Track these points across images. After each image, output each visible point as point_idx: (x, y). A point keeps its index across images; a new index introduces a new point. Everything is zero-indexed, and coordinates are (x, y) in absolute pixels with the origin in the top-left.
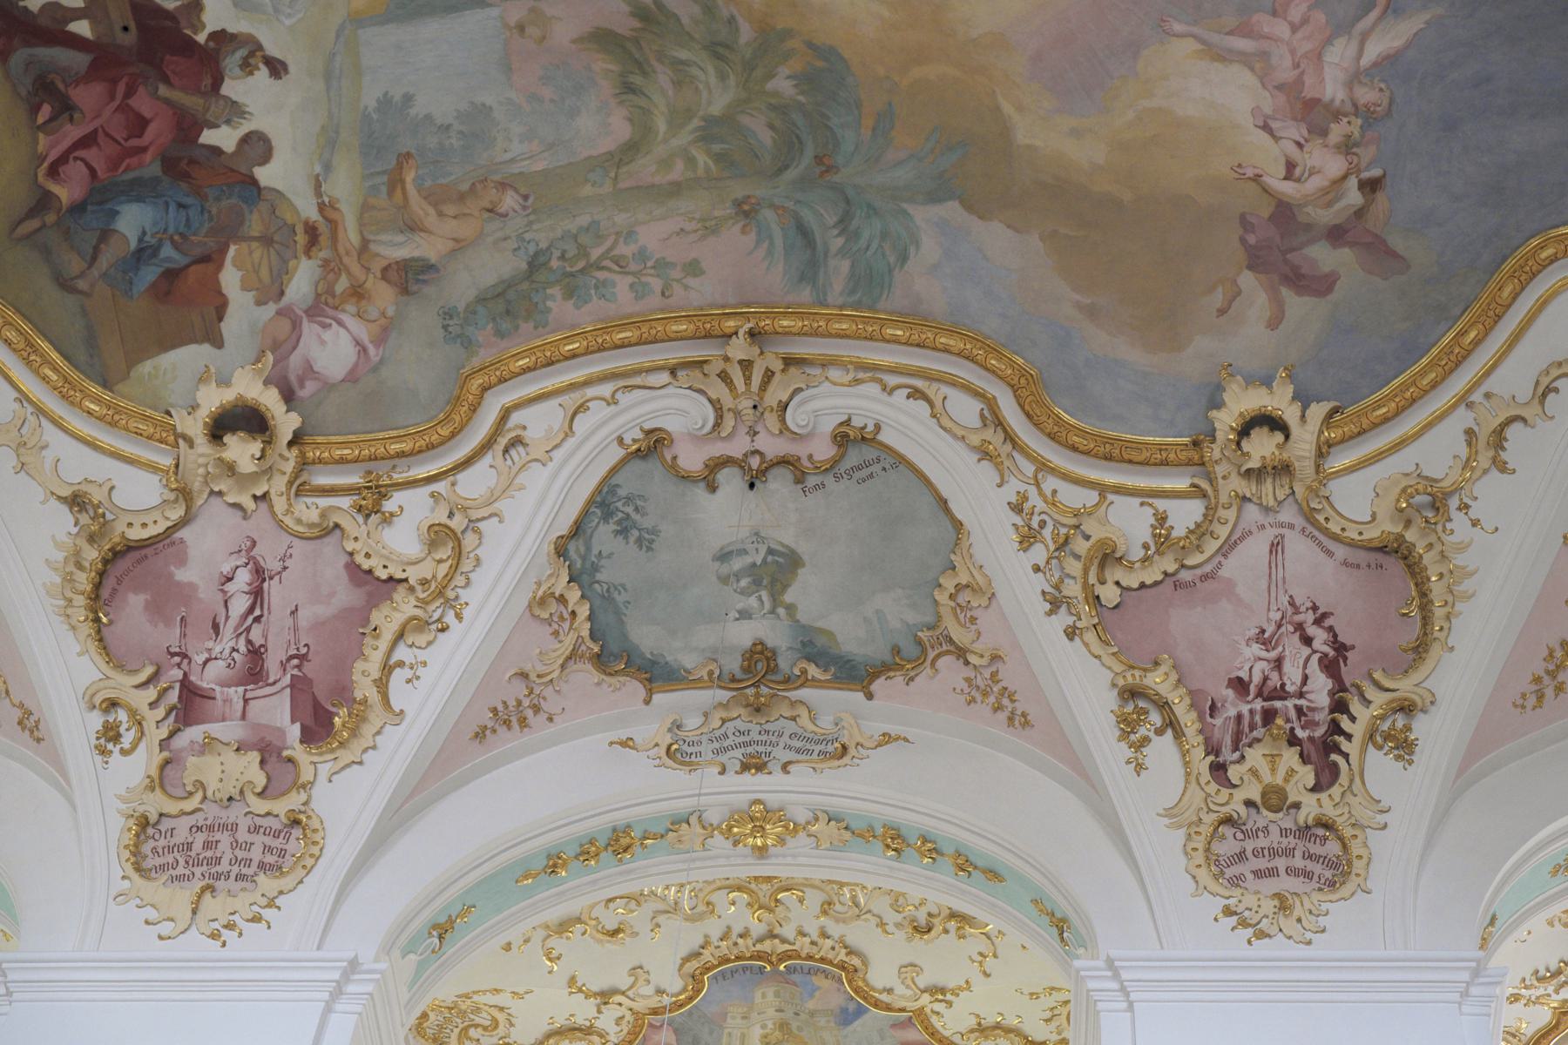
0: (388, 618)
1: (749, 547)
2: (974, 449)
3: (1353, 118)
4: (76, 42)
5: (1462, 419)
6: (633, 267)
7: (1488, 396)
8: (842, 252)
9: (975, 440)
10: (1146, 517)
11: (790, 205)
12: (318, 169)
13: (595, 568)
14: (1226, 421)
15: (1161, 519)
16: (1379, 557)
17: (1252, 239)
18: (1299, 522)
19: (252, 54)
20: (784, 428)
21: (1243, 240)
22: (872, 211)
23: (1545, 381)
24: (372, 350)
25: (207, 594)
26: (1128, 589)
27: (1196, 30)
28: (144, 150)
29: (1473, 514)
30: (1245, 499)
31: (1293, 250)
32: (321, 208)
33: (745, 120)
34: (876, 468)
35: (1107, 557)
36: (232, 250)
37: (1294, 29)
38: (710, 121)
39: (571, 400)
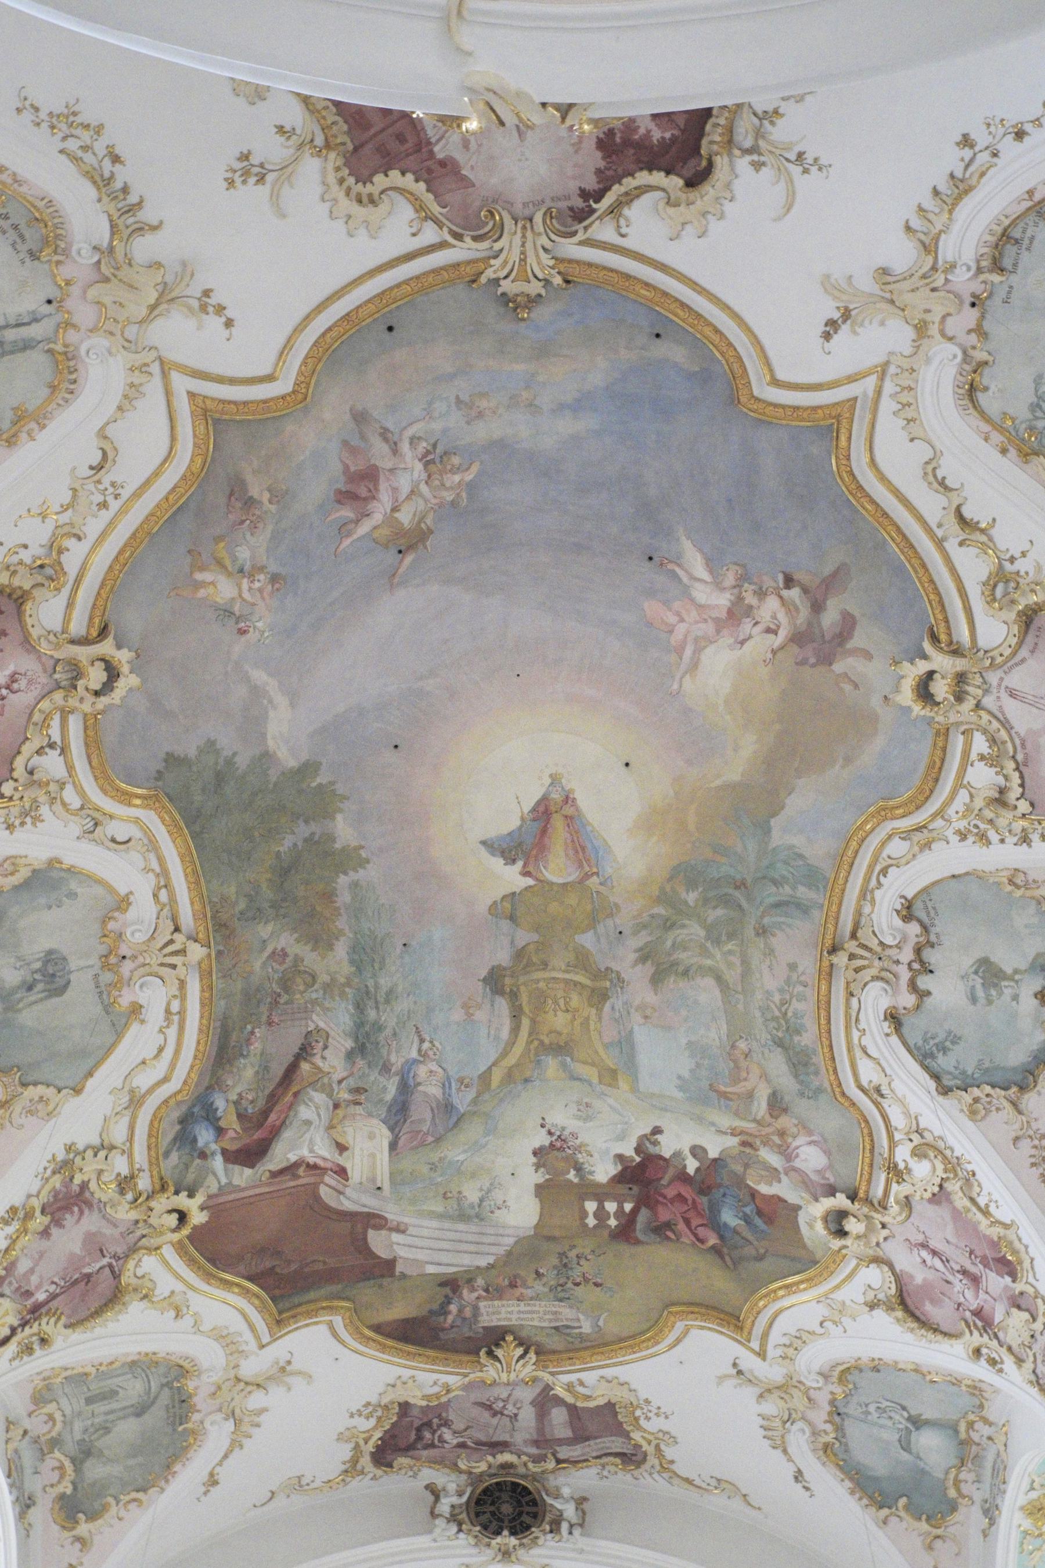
0: (961, 1202)
1: (971, 983)
2: (921, 850)
3: (743, 589)
4: (635, 1211)
5: (951, 546)
7: (940, 526)
8: (794, 888)
9: (916, 849)
10: (980, 766)
11: (761, 909)
12: (713, 1129)
13: (964, 1073)
14: (918, 709)
15: (982, 758)
16: (1033, 627)
17: (812, 660)
18: (999, 673)
20: (898, 946)
21: (813, 666)
22: (771, 866)
23: (936, 485)
25: (930, 1275)
26: (1023, 795)
28: (694, 1201)
29: (1017, 555)
30: (978, 706)
32: (733, 1134)
33: (709, 920)
34: (930, 904)
35: (1000, 799)
37: (682, 620)
38: (708, 938)
39: (858, 1053)
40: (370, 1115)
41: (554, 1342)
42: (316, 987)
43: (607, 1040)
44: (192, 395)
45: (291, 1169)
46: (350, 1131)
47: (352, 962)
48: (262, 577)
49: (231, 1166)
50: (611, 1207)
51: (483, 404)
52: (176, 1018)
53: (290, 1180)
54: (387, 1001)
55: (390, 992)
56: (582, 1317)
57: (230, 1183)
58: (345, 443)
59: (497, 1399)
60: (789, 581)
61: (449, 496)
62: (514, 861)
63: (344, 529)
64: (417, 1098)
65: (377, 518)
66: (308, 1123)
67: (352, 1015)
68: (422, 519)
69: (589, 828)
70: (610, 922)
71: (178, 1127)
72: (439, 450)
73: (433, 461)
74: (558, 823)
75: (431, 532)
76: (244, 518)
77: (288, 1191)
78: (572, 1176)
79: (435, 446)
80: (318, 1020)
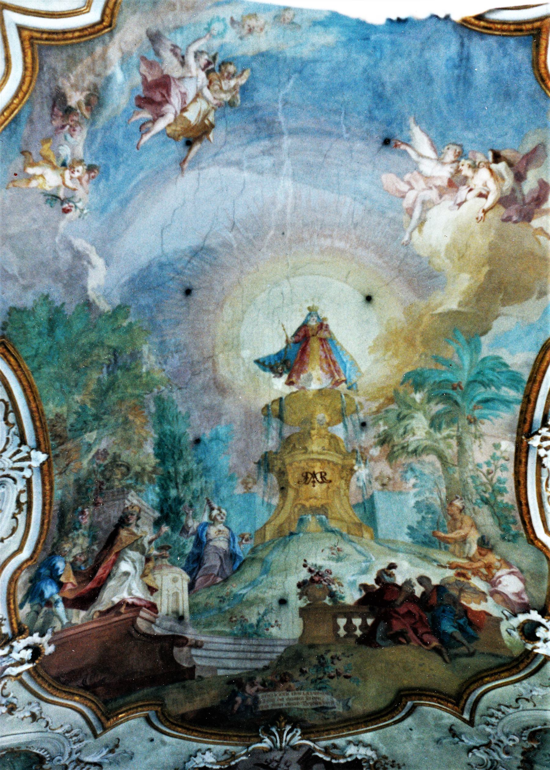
3: (461, 163)
6: (492, 468)
11: (473, 404)
12: (435, 564)
17: (515, 218)
19: (386, 573)
21: (516, 222)
24: (512, 570)
27: (409, 230)
31: (524, 200)
32: (451, 568)
36: (463, 602)
37: (412, 188)
40: (173, 564)
41: (315, 719)
42: (131, 475)
43: (354, 502)
44: (20, 29)
45: (115, 608)
46: (158, 577)
47: (157, 455)
48: (80, 168)
49: (70, 610)
50: (357, 622)
51: (252, 23)
52: (25, 507)
53: (115, 616)
54: (185, 482)
55: (186, 476)
56: (335, 700)
57: (70, 622)
58: (143, 58)
59: (272, 761)
60: (497, 157)
61: (226, 97)
62: (281, 375)
63: (143, 128)
64: (209, 550)
65: (170, 118)
66: (127, 574)
67: (158, 494)
68: (206, 116)
69: (338, 347)
70: (355, 417)
71: (30, 585)
72: (219, 60)
73: (213, 70)
74: (315, 344)
75: (212, 126)
76: (65, 123)
77: (114, 624)
78: (327, 601)
79: (214, 58)
80: (133, 499)
